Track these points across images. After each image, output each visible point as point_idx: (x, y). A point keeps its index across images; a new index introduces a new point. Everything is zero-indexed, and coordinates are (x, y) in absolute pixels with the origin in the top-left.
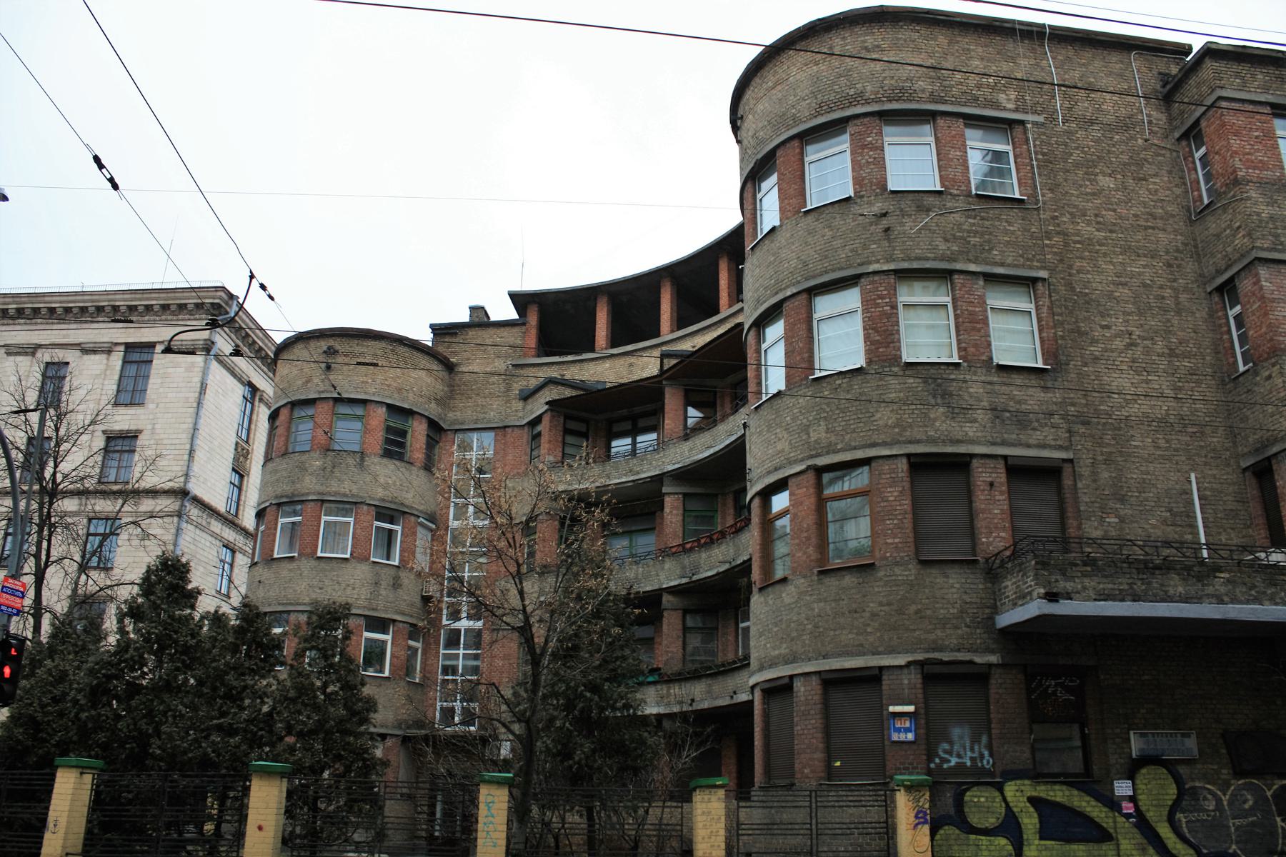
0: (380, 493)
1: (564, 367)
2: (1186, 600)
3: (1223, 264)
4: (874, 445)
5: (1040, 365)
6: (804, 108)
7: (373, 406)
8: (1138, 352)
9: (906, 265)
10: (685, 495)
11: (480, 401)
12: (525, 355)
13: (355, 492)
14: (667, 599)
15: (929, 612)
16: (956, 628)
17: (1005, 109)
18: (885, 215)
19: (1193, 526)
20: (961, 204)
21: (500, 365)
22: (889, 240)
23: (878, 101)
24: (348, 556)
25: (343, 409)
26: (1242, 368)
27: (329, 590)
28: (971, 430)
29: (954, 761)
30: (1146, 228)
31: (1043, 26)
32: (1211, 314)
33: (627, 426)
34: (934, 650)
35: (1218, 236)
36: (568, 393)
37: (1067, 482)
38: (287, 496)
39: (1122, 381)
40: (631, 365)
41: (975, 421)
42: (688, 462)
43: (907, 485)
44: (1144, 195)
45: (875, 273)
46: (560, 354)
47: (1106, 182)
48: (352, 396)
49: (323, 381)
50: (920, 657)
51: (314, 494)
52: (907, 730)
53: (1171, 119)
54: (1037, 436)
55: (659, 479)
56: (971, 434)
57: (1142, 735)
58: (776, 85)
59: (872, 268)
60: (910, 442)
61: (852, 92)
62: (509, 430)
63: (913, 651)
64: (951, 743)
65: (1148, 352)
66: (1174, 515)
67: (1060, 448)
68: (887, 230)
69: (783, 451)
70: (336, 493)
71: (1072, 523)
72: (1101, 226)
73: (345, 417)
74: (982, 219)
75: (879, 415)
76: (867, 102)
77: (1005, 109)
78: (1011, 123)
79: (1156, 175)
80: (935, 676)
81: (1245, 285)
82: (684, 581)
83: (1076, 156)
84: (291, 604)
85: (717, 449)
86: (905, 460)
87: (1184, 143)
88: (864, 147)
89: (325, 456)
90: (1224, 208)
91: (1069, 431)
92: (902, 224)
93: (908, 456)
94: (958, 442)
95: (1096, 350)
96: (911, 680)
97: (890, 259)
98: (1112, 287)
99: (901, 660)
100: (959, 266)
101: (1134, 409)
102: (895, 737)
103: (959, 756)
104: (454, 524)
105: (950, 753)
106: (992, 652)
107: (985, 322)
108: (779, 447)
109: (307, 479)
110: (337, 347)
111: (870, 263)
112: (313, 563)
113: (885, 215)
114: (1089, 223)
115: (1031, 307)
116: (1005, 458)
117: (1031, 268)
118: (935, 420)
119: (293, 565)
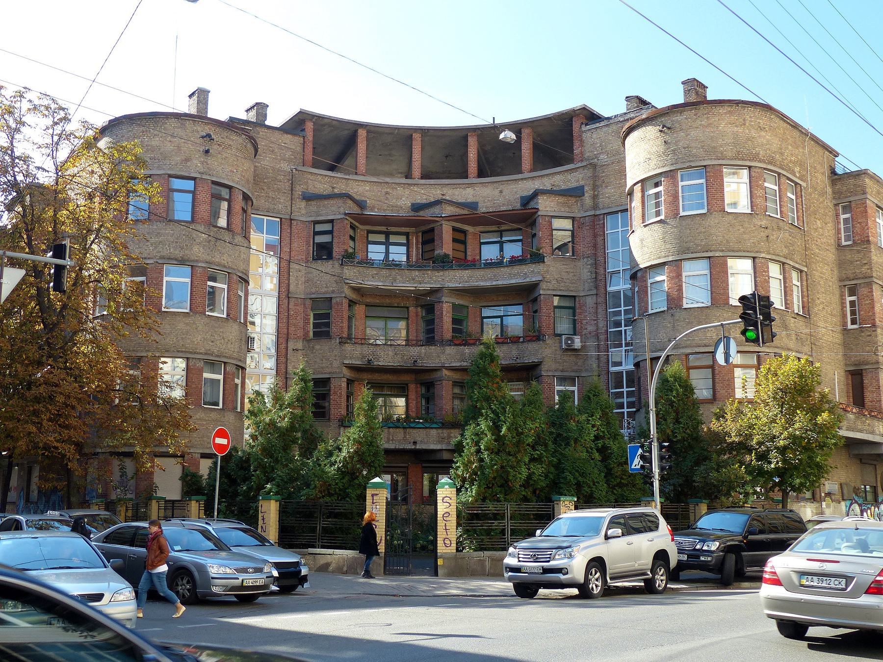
2: (861, 431)
3: (852, 276)
8: (824, 312)
9: (774, 257)
10: (454, 304)
13: (230, 264)
21: (286, 167)
23: (765, 162)
26: (850, 326)
33: (381, 238)
35: (851, 262)
39: (821, 324)
42: (466, 285)
49: (202, 163)
53: (834, 193)
55: (433, 292)
58: (709, 125)
59: (763, 255)
76: (760, 161)
81: (863, 291)
82: (465, 364)
84: (191, 353)
85: (500, 283)
90: (859, 252)
107: (768, 282)
109: (196, 249)
110: (213, 136)
112: (206, 320)
115: (781, 277)
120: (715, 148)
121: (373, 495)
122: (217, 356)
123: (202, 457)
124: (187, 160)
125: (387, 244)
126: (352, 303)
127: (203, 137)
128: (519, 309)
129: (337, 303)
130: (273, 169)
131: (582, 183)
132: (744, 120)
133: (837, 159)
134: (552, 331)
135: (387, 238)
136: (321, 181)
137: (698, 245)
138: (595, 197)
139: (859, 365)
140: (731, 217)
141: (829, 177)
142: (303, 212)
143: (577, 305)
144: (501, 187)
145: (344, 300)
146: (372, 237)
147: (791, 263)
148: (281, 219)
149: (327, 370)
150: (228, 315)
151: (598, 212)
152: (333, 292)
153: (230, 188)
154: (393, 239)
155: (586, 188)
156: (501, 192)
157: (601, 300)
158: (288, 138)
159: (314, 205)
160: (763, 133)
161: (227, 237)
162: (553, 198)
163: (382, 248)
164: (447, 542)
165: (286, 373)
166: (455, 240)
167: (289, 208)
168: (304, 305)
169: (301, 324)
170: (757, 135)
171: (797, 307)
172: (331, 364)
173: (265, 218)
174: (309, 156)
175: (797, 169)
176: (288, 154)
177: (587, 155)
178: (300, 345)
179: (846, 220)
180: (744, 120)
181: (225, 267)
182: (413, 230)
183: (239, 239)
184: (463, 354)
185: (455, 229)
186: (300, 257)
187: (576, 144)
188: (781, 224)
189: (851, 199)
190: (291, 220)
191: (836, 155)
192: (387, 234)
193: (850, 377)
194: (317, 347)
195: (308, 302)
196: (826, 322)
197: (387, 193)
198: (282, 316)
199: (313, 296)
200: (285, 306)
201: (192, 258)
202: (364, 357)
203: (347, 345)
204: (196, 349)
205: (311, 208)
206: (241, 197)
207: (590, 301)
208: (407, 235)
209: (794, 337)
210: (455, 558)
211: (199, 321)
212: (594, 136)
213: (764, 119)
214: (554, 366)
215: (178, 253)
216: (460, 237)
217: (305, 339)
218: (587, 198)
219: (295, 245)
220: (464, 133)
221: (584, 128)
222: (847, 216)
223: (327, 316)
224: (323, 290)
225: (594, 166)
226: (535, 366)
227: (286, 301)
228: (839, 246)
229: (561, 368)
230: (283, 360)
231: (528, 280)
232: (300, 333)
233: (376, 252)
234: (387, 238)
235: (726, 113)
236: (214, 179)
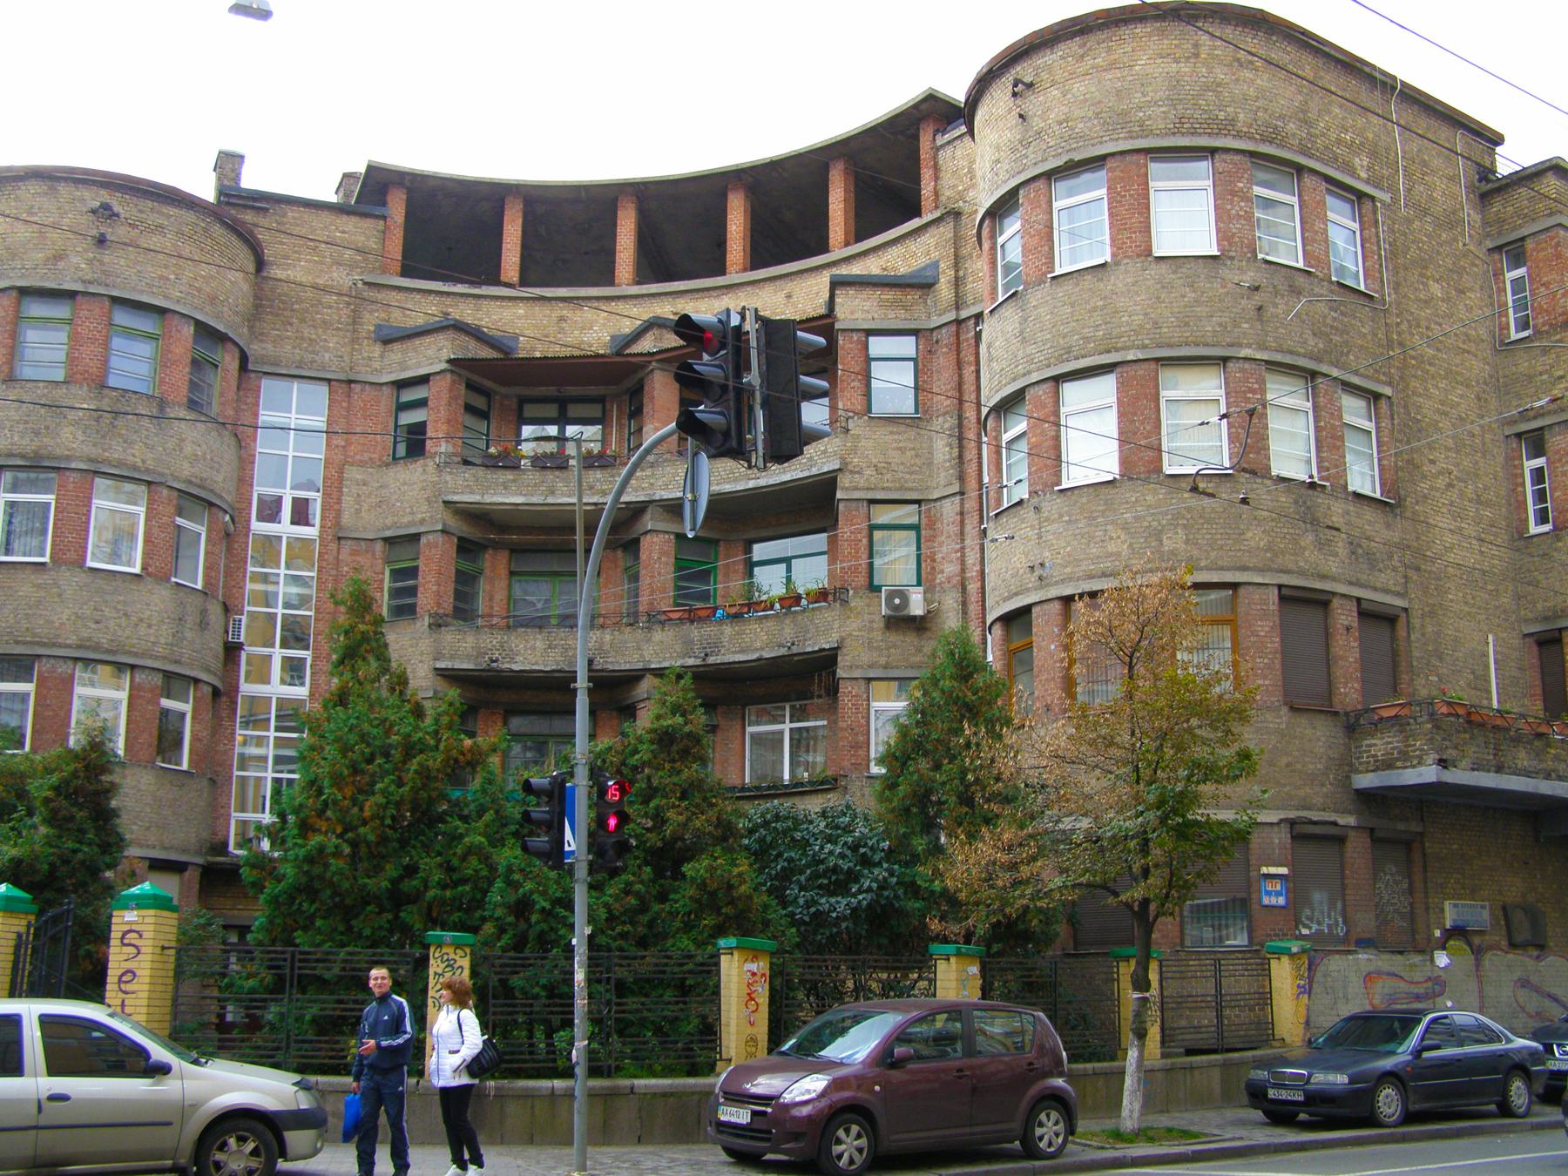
0: (186, 470)
1: (449, 301)
2: (1527, 773)
4: (1244, 569)
5: (1378, 495)
6: (1158, 117)
7: (176, 320)
8: (1454, 495)
9: (1278, 358)
11: (307, 332)
12: (384, 270)
13: (151, 464)
14: (646, 685)
15: (1299, 766)
16: (1323, 785)
17: (1359, 178)
18: (1257, 289)
19: (1489, 692)
20: (1323, 290)
21: (342, 278)
22: (1260, 319)
24: (46, 559)
25: (122, 318)
27: (112, 624)
28: (1333, 566)
29: (1315, 927)
30: (1464, 351)
31: (1394, 78)
32: (1508, 459)
33: (552, 410)
34: (1305, 808)
35: (1530, 378)
36: (486, 353)
37: (1401, 632)
38: (23, 457)
39: (1443, 522)
40: (562, 319)
41: (1336, 555)
43: (1277, 619)
44: (1463, 314)
45: (1245, 359)
46: (472, 283)
47: (1436, 289)
48: (145, 299)
49: (90, 262)
50: (1292, 815)
51: (81, 459)
52: (1278, 894)
53: (1485, 223)
54: (1383, 579)
56: (1326, 566)
57: (1455, 906)
60: (1282, 571)
61: (1222, 115)
62: (357, 388)
63: (1284, 808)
64: (1313, 910)
65: (1461, 495)
66: (1476, 678)
67: (1398, 594)
68: (1260, 309)
69: (1119, 554)
70: (120, 464)
71: (1405, 677)
72: (1431, 342)
73: (130, 333)
74: (1342, 314)
75: (1249, 534)
77: (1359, 178)
78: (1361, 196)
79: (1471, 290)
80: (1303, 834)
83: (1413, 252)
84: (44, 645)
86: (1276, 591)
87: (1496, 256)
88: (1233, 193)
90: (1545, 351)
91: (1406, 577)
92: (1276, 306)
93: (1280, 587)
94: (1323, 577)
95: (1424, 486)
96: (1281, 837)
97: (1262, 347)
98: (1437, 417)
99: (1272, 817)
100: (1324, 369)
101: (1451, 557)
102: (1266, 901)
103: (1319, 923)
104: (258, 527)
105: (1311, 919)
106: (1350, 813)
108: (1112, 547)
109: (66, 433)
110: (117, 208)
111: (1240, 345)
112: (83, 578)
113: (1257, 289)
114: (1422, 336)
116: (1359, 600)
117: (1378, 381)
118: (1305, 549)
120: (1124, 113)
122: (108, 651)
124: (58, 258)
126: (466, 548)
127: (93, 212)
129: (429, 544)
131: (935, 255)
132: (1196, 46)
133: (1498, 149)
134: (862, 580)
137: (1087, 339)
138: (958, 282)
139: (1556, 617)
140: (1163, 266)
141: (1470, 188)
142: (377, 365)
143: (924, 521)
144: (789, 286)
145: (440, 538)
147: (1335, 373)
151: (964, 314)
152: (422, 521)
154: (574, 410)
156: (789, 297)
157: (971, 504)
158: (350, 224)
159: (396, 353)
160: (1248, 74)
162: (868, 292)
170: (1227, 79)
171: (1362, 477)
175: (1361, 162)
177: (947, 193)
179: (1518, 284)
180: (1196, 46)
181: (135, 468)
182: (612, 389)
184: (688, 643)
186: (366, 456)
187: (926, 175)
188: (1301, 280)
189: (1525, 232)
191: (1496, 139)
193: (1535, 649)
195: (379, 546)
196: (1457, 516)
197: (562, 319)
199: (388, 534)
201: (58, 452)
202: (481, 654)
204: (57, 636)
206: (189, 330)
207: (949, 509)
209: (1341, 549)
211: (69, 580)
212: (958, 153)
214: (865, 658)
215: (27, 444)
218: (944, 290)
221: (940, 140)
222: (1521, 272)
223: (413, 572)
224: (405, 520)
225: (957, 214)
227: (334, 546)
228: (1502, 343)
229: (883, 660)
231: (814, 471)
235: (1150, 35)
236: (115, 293)
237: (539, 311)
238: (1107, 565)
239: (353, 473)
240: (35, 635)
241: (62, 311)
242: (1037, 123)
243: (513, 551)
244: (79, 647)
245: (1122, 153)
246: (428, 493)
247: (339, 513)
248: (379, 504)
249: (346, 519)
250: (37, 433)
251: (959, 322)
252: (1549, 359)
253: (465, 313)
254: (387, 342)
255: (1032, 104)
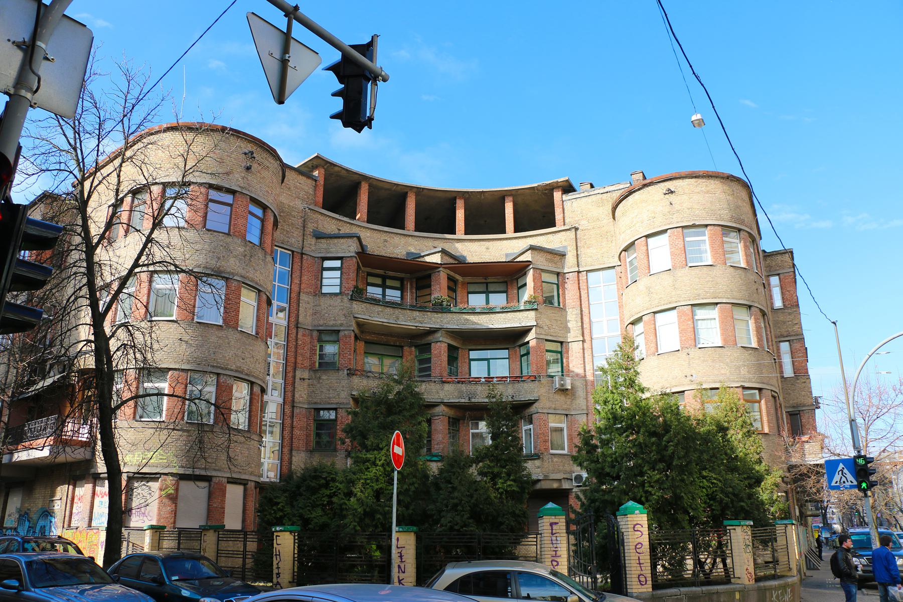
10: (449, 345)
14: (441, 409)
27: (248, 360)
33: (378, 281)
35: (784, 323)
55: (432, 331)
70: (252, 281)
82: (463, 401)
84: (222, 368)
89: (246, 245)
90: (790, 314)
108: (723, 372)
109: (232, 260)
112: (238, 335)
119: (222, 333)
121: (551, 524)
122: (247, 374)
123: (228, 482)
125: (384, 286)
126: (356, 338)
127: (245, 154)
128: (505, 353)
129: (345, 336)
130: (289, 206)
131: (565, 244)
135: (384, 282)
136: (330, 223)
142: (313, 248)
146: (371, 280)
148: (293, 252)
149: (335, 401)
150: (257, 333)
152: (341, 325)
153: (264, 208)
154: (389, 282)
155: (569, 248)
158: (302, 179)
159: (323, 244)
161: (260, 254)
162: (542, 254)
163: (379, 290)
164: (643, 579)
165: (293, 401)
166: (449, 288)
167: (301, 242)
168: (312, 336)
169: (308, 355)
172: (338, 395)
173: (279, 249)
174: (320, 199)
176: (302, 193)
178: (306, 375)
181: (257, 283)
183: (269, 258)
185: (450, 279)
186: (309, 290)
190: (302, 254)
192: (384, 278)
194: (324, 377)
195: (315, 334)
197: (386, 241)
198: (290, 345)
199: (321, 328)
200: (293, 336)
203: (354, 377)
204: (228, 364)
205: (321, 245)
208: (402, 280)
210: (653, 597)
211: (232, 335)
213: (744, 194)
214: (548, 404)
216: (452, 284)
217: (312, 369)
219: (305, 278)
220: (454, 195)
221: (565, 197)
224: (331, 323)
225: (576, 229)
226: (529, 404)
227: (294, 331)
230: (290, 388)
232: (307, 363)
233: (374, 291)
234: (384, 282)
237: (376, 235)
238: (721, 378)
239: (303, 297)
240: (218, 363)
241: (229, 198)
242: (677, 207)
243: (366, 342)
244: (236, 371)
245: (714, 225)
246: (345, 312)
247: (298, 316)
248: (315, 314)
249: (301, 319)
250: (219, 258)
251: (579, 272)
252: (792, 317)
253: (346, 229)
254: (318, 238)
255: (671, 197)
